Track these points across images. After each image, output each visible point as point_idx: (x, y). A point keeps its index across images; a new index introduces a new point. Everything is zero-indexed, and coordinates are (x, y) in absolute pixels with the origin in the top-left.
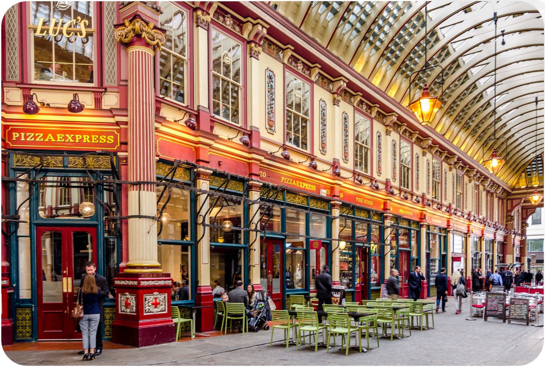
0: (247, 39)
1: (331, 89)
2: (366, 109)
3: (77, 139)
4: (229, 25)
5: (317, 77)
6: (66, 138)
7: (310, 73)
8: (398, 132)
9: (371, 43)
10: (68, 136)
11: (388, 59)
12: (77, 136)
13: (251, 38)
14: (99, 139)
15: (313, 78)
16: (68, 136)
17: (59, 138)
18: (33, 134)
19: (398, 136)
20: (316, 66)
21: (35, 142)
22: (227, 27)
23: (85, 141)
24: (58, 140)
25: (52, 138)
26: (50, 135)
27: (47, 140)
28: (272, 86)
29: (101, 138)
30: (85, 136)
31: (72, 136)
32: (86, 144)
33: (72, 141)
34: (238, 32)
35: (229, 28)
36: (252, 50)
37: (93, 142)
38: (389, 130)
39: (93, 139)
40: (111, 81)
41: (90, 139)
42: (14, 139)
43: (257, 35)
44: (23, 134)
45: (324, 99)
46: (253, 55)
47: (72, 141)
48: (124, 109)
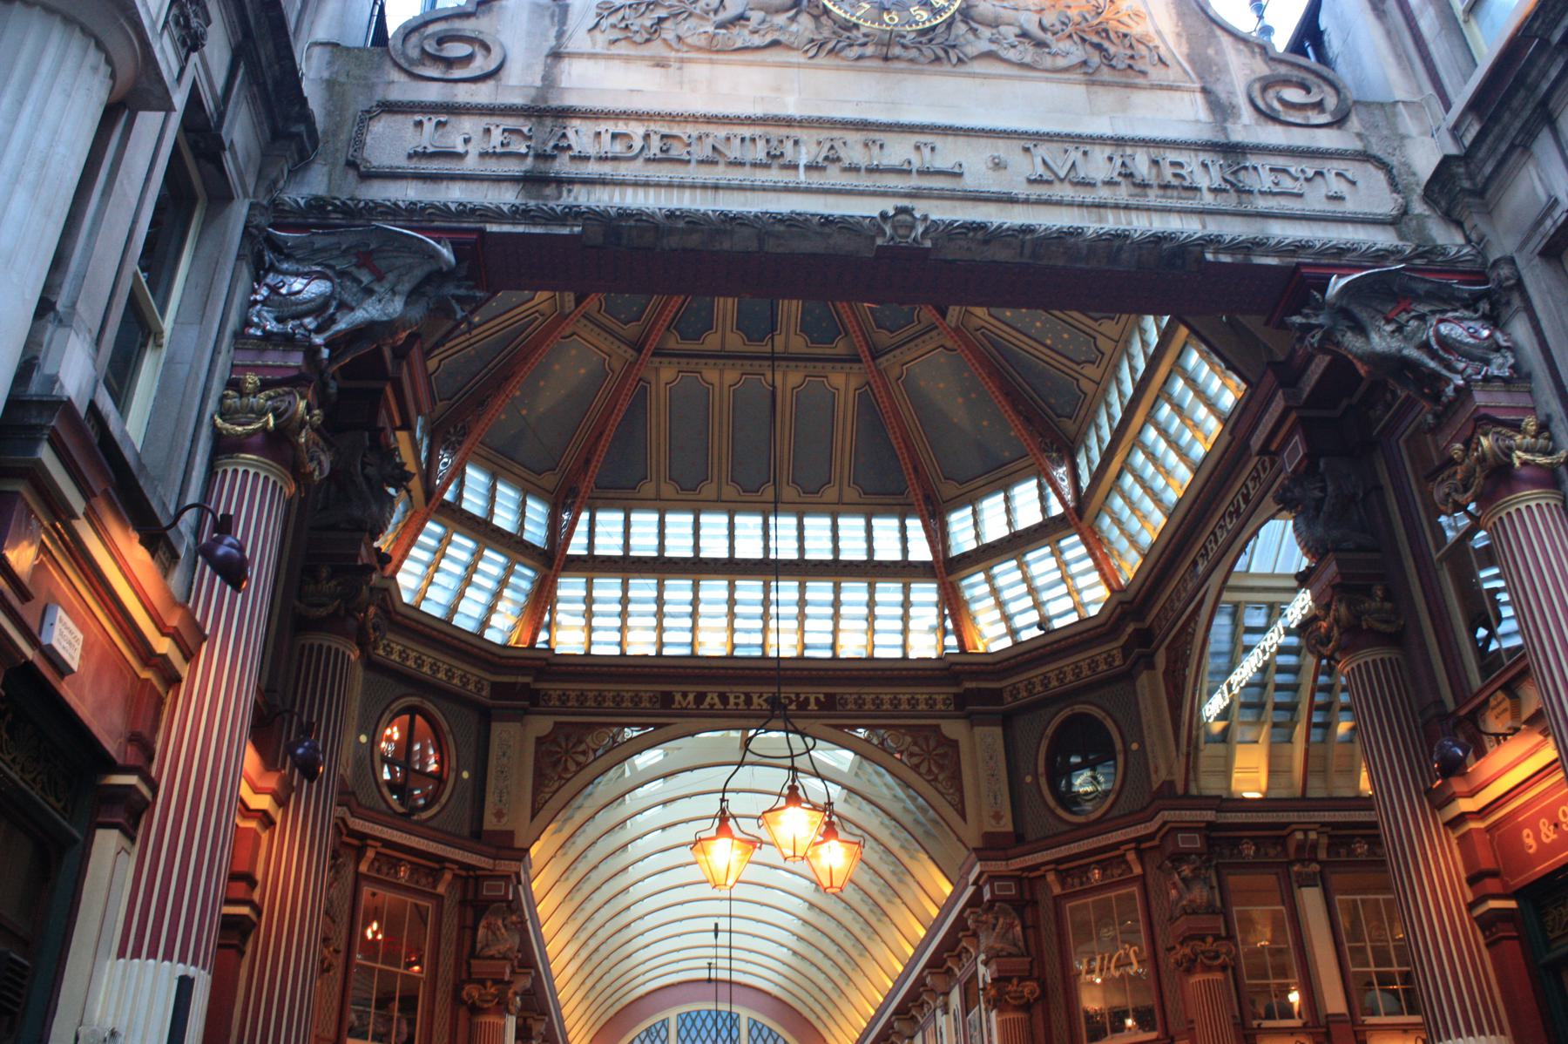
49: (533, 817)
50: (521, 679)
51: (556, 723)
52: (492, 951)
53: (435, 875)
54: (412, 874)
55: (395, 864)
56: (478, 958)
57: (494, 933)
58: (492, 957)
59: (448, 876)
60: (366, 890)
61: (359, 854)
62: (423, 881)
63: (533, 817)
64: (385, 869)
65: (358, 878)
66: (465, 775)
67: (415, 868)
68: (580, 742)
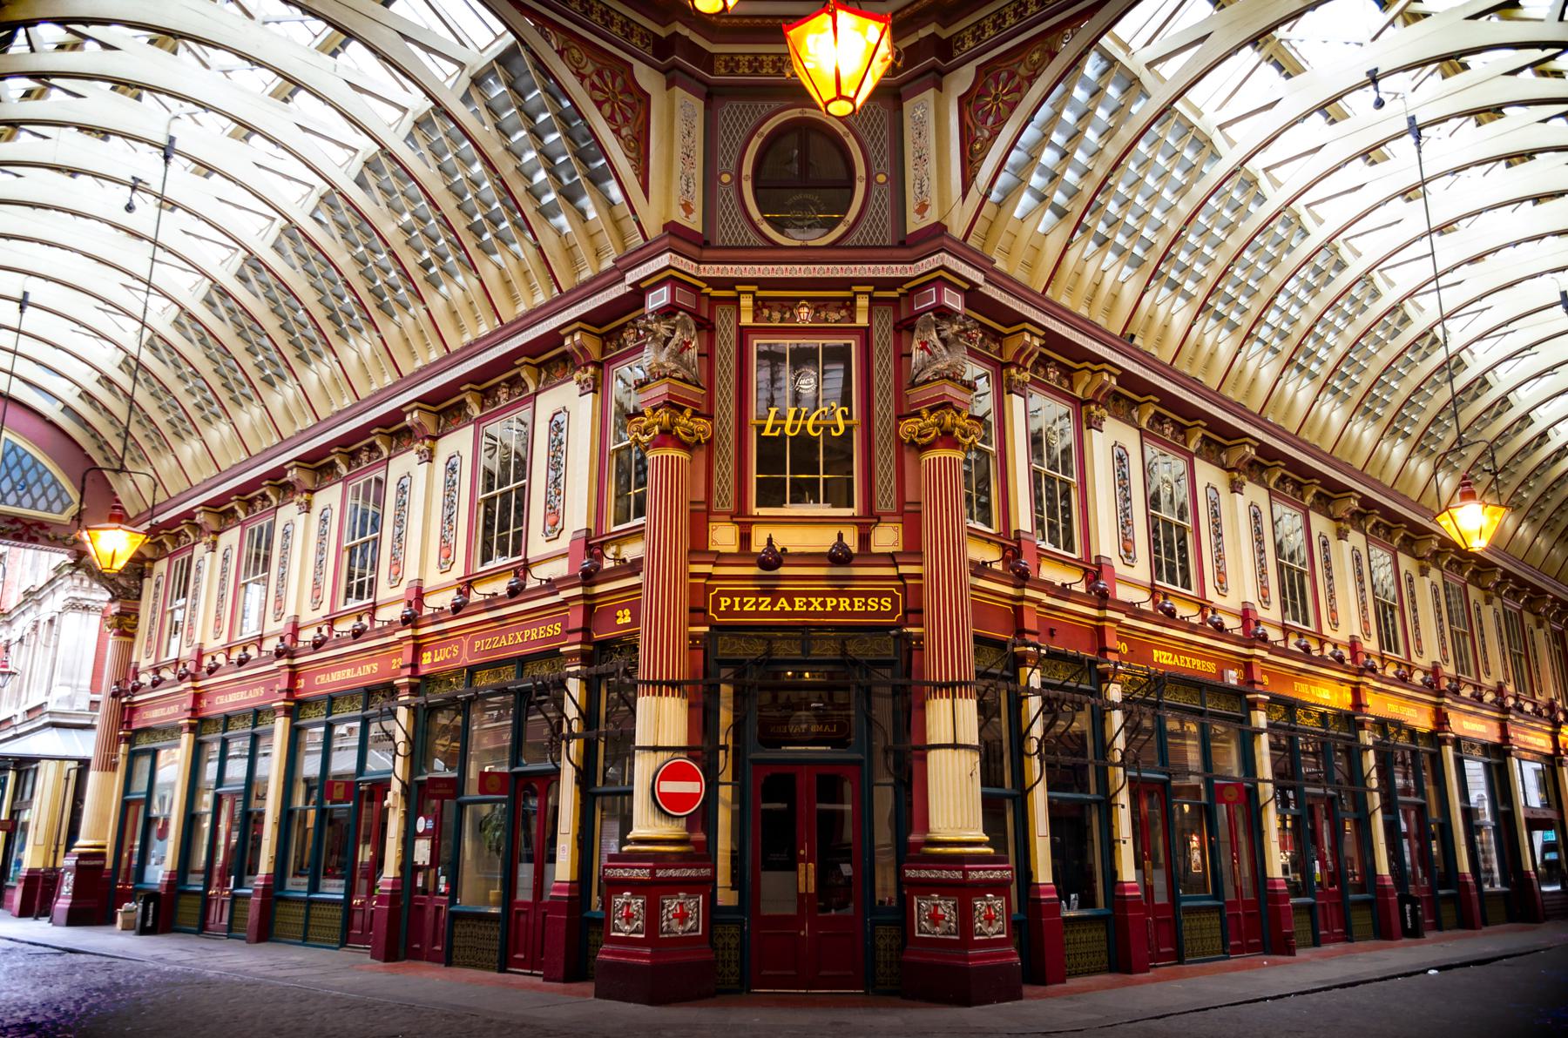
3: (829, 604)
6: (809, 604)
10: (813, 600)
12: (828, 600)
14: (866, 604)
16: (813, 600)
17: (797, 604)
18: (754, 600)
21: (757, 614)
23: (841, 609)
24: (797, 609)
25: (786, 604)
26: (783, 600)
27: (777, 609)
29: (869, 601)
30: (841, 600)
31: (820, 599)
32: (845, 614)
33: (819, 609)
37: (856, 609)
39: (856, 604)
40: (886, 504)
41: (852, 605)
42: (722, 609)
44: (737, 600)
47: (819, 609)
48: (913, 548)
49: (964, 195)
50: (923, 33)
51: (979, 68)
52: (928, 374)
53: (849, 305)
54: (817, 310)
55: (790, 304)
56: (913, 385)
57: (930, 353)
58: (927, 381)
59: (862, 302)
60: (757, 343)
61: (736, 301)
62: (837, 317)
63: (964, 195)
64: (776, 315)
65: (743, 333)
66: (881, 178)
67: (819, 305)
68: (1012, 76)
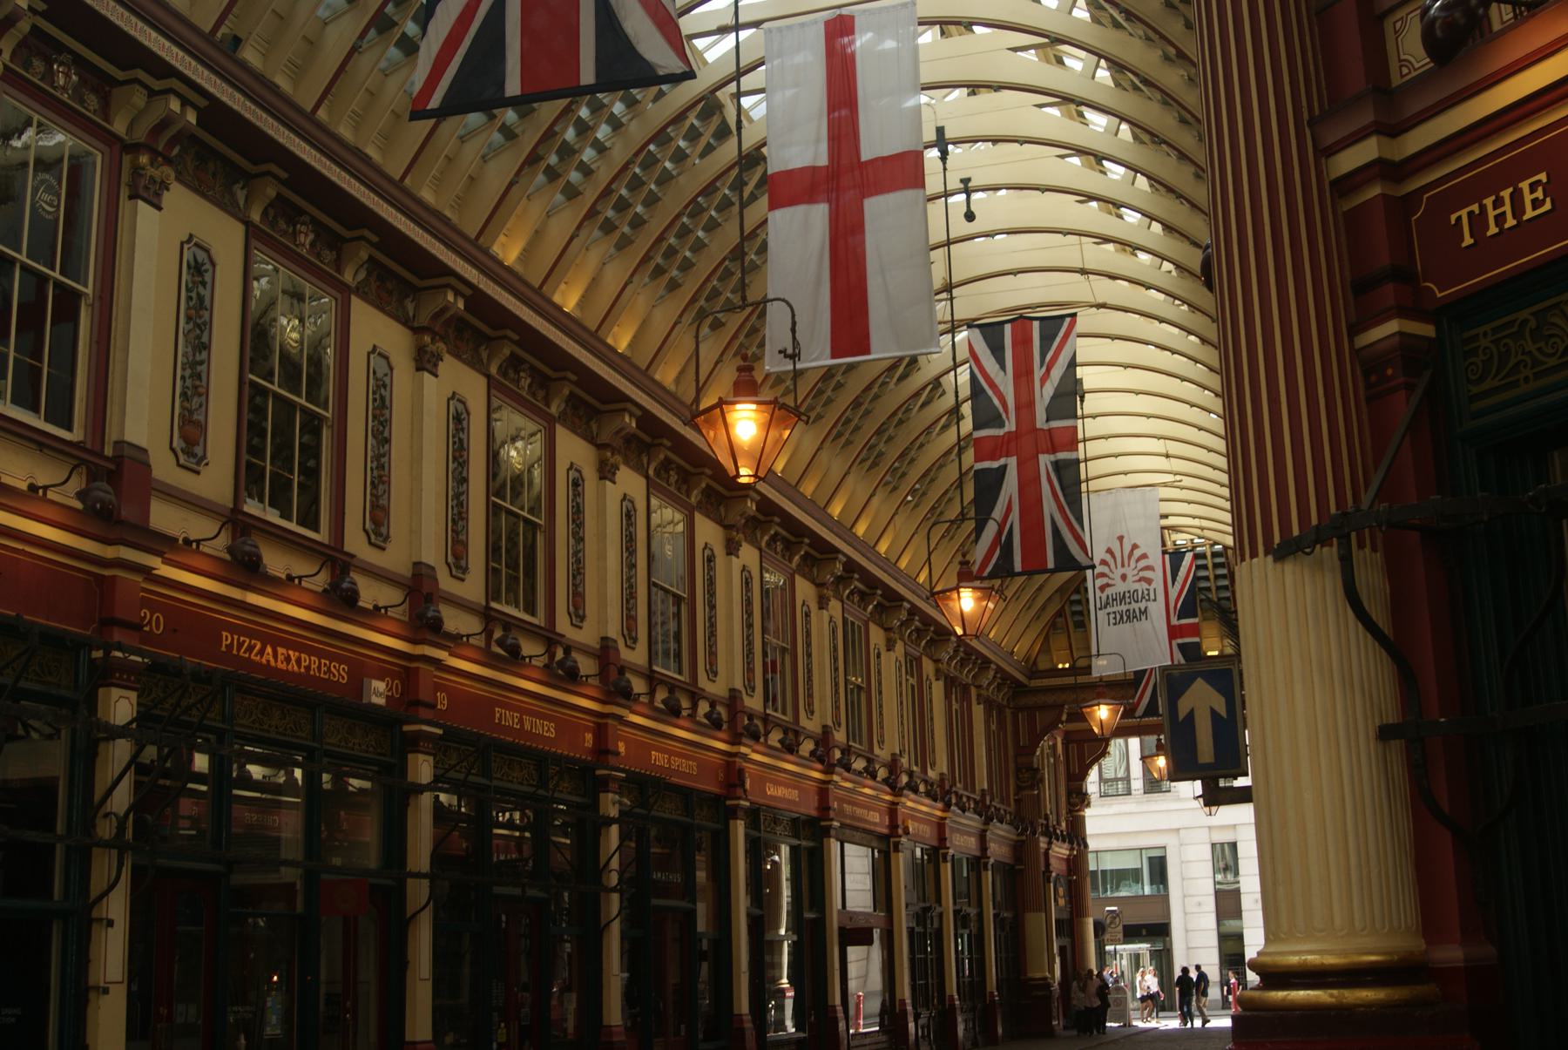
0: (126, 138)
1: (411, 314)
2: (530, 386)
4: (64, 89)
5: (362, 275)
7: (547, 394)
8: (641, 470)
9: (552, 174)
11: (608, 227)
13: (140, 134)
15: (348, 277)
19: (643, 481)
20: (565, 378)
22: (58, 94)
28: (201, 298)
34: (95, 112)
35: (65, 97)
36: (141, 175)
38: (612, 460)
43: (164, 124)
45: (384, 347)
46: (142, 192)
